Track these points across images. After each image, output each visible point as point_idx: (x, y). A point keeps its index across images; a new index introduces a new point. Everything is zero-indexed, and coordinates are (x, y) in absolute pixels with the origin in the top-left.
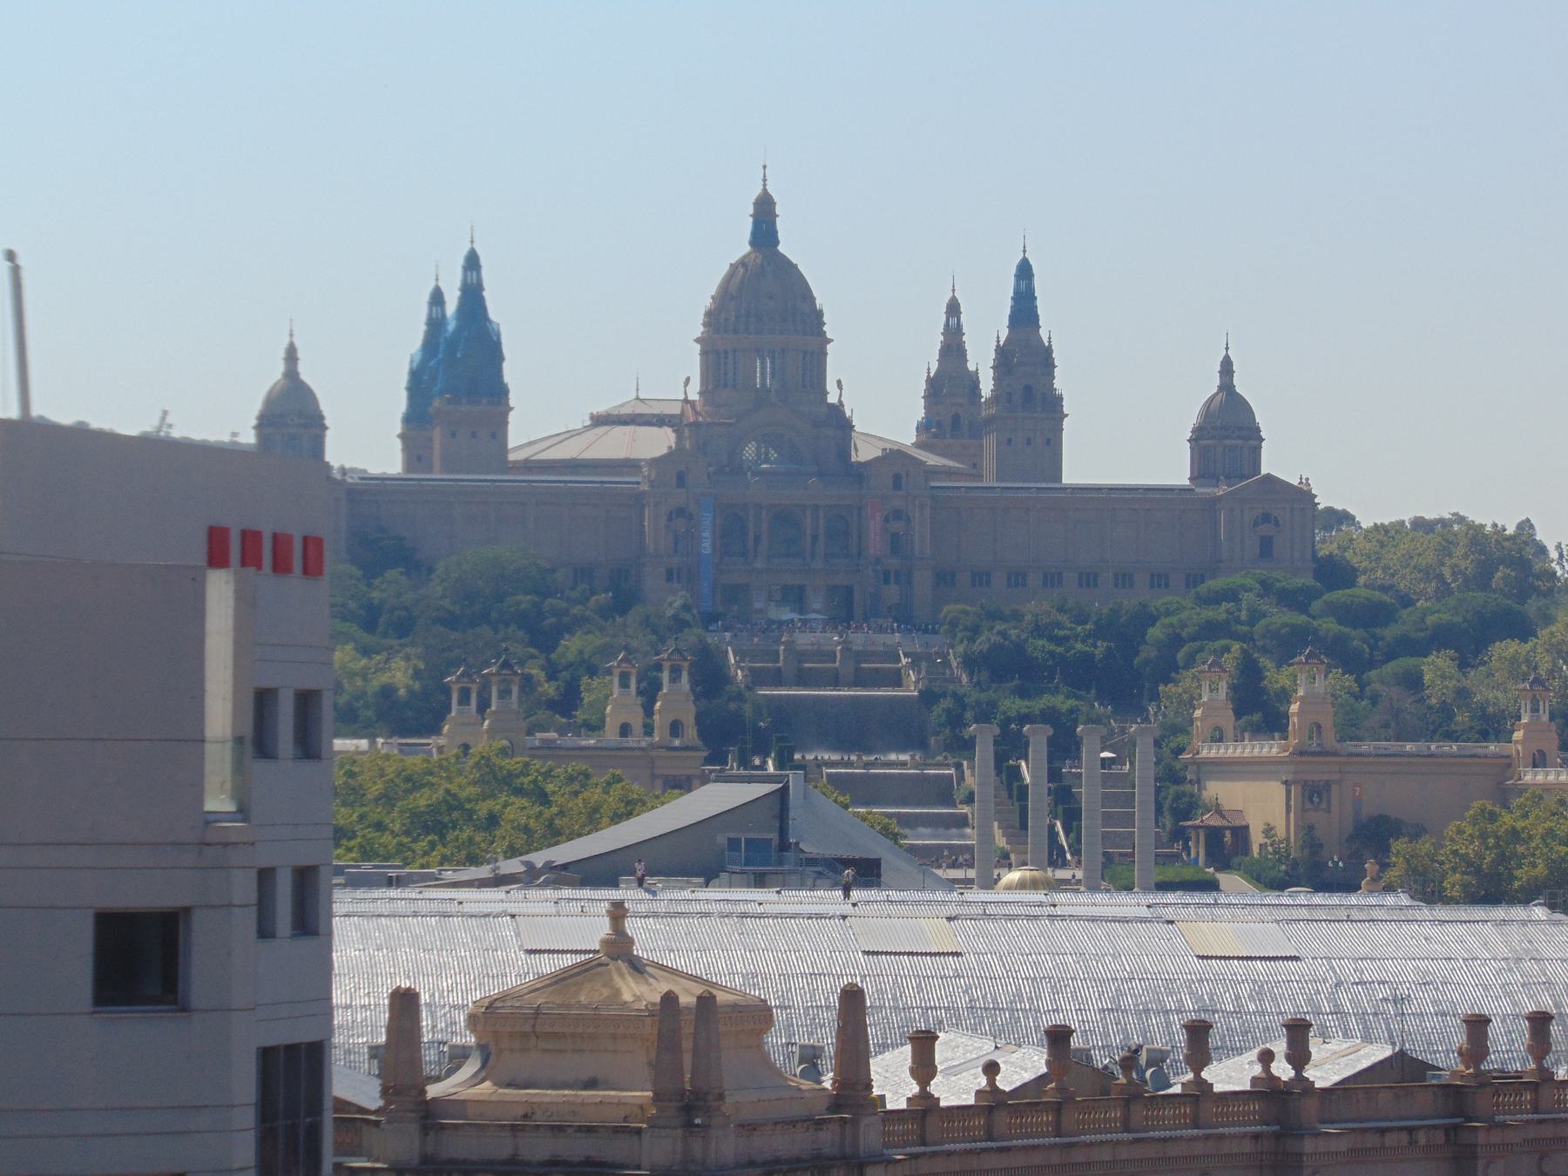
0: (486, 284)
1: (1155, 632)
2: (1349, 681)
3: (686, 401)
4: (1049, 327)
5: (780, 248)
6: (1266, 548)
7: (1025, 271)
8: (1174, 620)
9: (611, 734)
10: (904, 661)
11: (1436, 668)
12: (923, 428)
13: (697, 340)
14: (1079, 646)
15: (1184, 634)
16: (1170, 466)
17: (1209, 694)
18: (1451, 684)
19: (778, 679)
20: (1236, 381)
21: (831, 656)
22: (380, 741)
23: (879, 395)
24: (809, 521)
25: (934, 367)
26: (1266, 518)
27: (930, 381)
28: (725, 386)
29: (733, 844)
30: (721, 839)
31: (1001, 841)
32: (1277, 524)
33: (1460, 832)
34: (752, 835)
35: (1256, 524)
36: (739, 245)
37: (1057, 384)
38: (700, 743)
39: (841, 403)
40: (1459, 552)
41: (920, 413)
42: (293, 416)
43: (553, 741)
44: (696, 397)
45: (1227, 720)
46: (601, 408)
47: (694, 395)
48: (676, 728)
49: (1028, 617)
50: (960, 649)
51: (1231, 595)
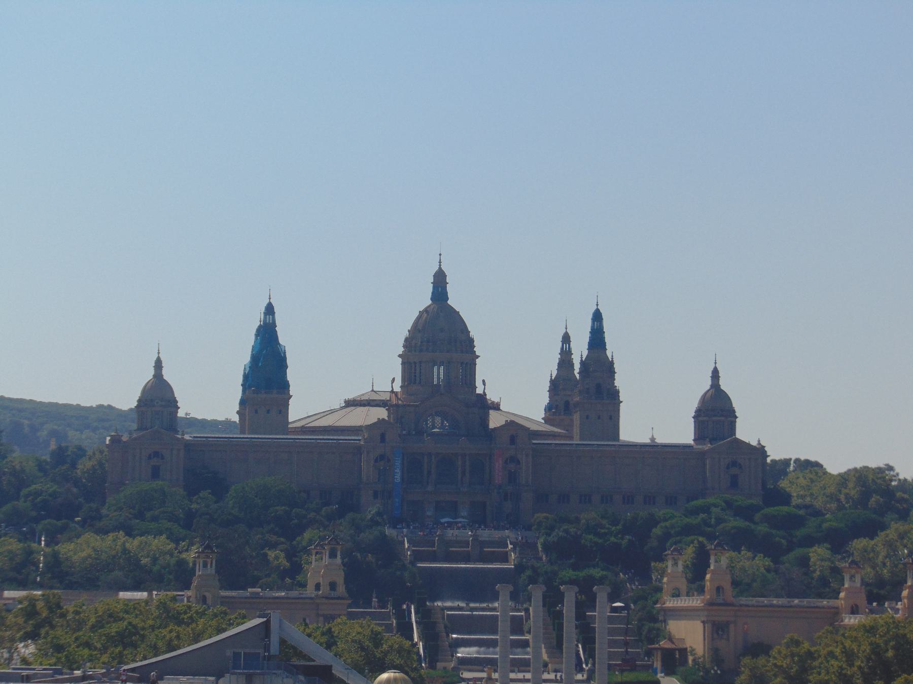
1: (657, 531)
2: (768, 562)
3: (392, 392)
4: (612, 349)
5: (449, 302)
6: (734, 483)
7: (597, 317)
8: (667, 524)
9: (310, 591)
10: (510, 546)
11: (818, 554)
12: (548, 409)
13: (400, 356)
14: (613, 539)
15: (672, 532)
16: (681, 432)
17: (672, 570)
18: (826, 564)
19: (434, 558)
21: (467, 544)
22: (155, 593)
24: (460, 463)
26: (734, 464)
27: (552, 381)
28: (415, 383)
29: (236, 655)
30: (229, 653)
31: (545, 657)
32: (741, 467)
33: (779, 652)
34: (247, 651)
35: (728, 468)
36: (424, 300)
37: (617, 383)
38: (346, 595)
39: (485, 394)
40: (851, 485)
41: (546, 400)
42: (158, 398)
43: (258, 593)
45: (683, 585)
46: (351, 396)
47: (397, 388)
48: (333, 586)
49: (583, 521)
50: (542, 540)
51: (706, 509)
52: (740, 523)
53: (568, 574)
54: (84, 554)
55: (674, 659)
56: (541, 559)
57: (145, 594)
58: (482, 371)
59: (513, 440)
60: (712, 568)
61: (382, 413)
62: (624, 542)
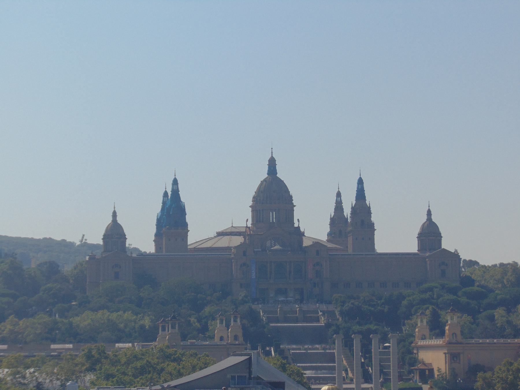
0: (180, 189)
1: (405, 302)
2: (469, 318)
3: (247, 227)
4: (369, 200)
5: (278, 175)
7: (360, 182)
9: (217, 340)
10: (320, 313)
11: (499, 313)
12: (329, 235)
16: (411, 247)
17: (421, 324)
18: (504, 319)
19: (278, 321)
20: (432, 217)
22: (136, 344)
23: (313, 223)
25: (333, 214)
27: (331, 219)
29: (233, 378)
30: (229, 376)
33: (500, 369)
36: (264, 174)
37: (372, 219)
40: (509, 274)
41: (328, 230)
42: (115, 234)
44: (250, 226)
45: (427, 332)
46: (220, 230)
47: (249, 225)
48: (236, 338)
49: (362, 298)
50: (339, 309)
51: (431, 289)
52: (452, 297)
53: (356, 328)
54: (86, 323)
55: (427, 374)
56: (338, 320)
57: (130, 345)
58: (297, 214)
59: (318, 253)
60: (449, 322)
61: (238, 241)
62: (386, 310)
